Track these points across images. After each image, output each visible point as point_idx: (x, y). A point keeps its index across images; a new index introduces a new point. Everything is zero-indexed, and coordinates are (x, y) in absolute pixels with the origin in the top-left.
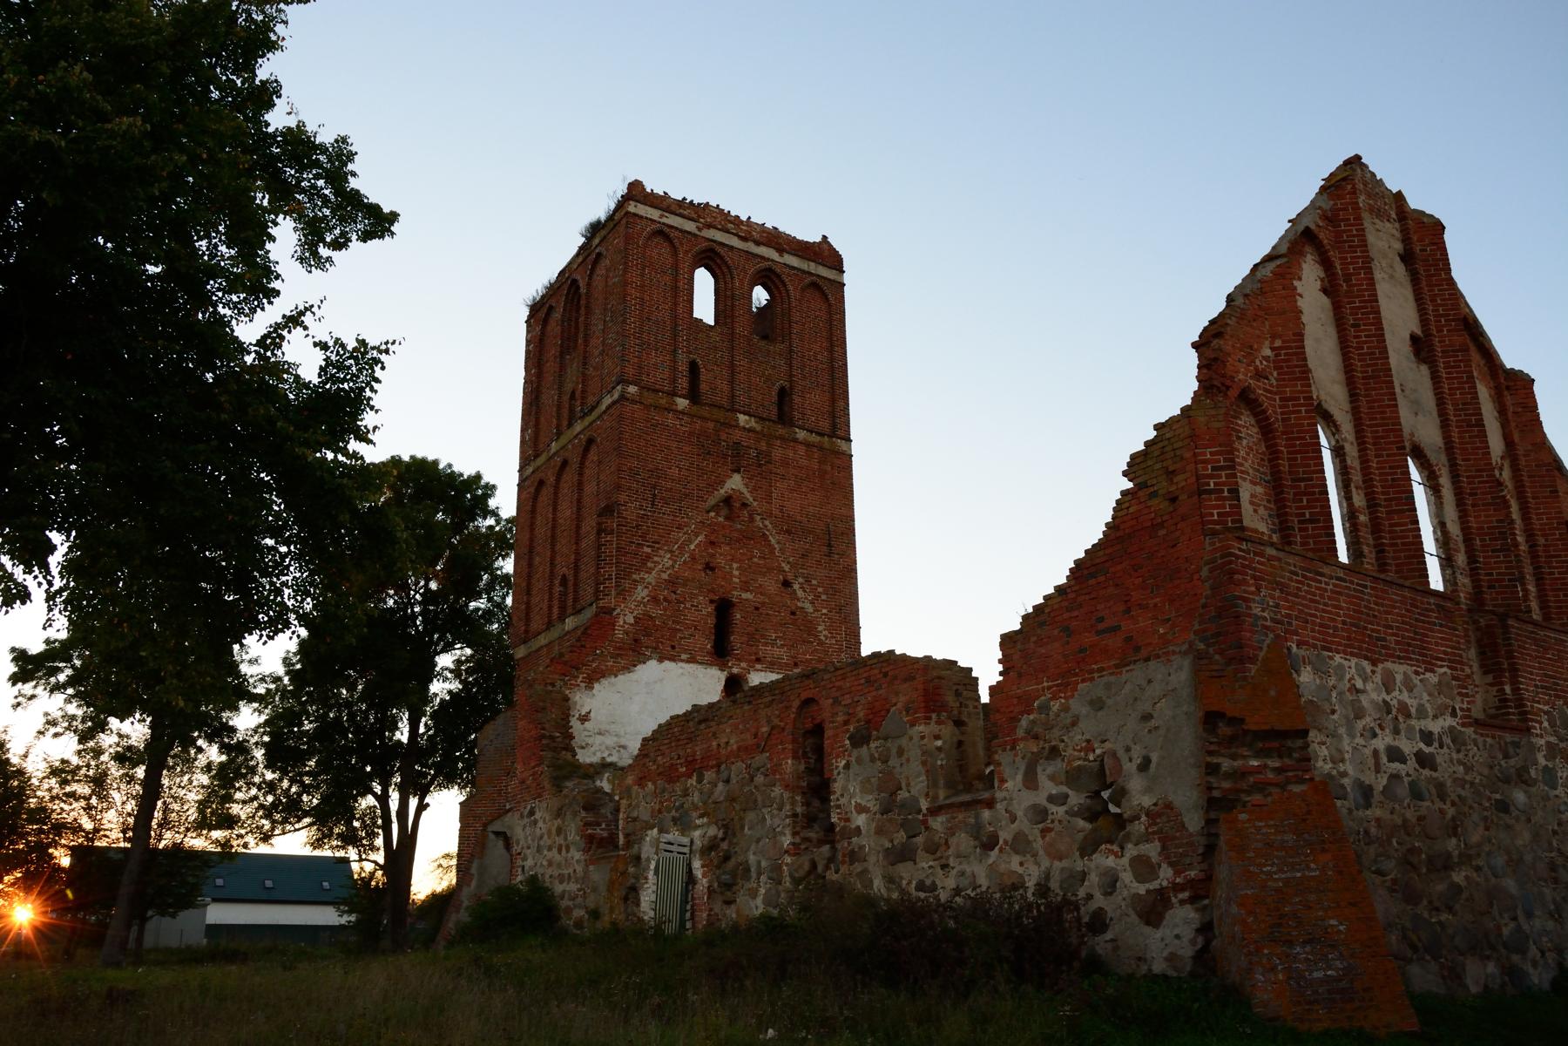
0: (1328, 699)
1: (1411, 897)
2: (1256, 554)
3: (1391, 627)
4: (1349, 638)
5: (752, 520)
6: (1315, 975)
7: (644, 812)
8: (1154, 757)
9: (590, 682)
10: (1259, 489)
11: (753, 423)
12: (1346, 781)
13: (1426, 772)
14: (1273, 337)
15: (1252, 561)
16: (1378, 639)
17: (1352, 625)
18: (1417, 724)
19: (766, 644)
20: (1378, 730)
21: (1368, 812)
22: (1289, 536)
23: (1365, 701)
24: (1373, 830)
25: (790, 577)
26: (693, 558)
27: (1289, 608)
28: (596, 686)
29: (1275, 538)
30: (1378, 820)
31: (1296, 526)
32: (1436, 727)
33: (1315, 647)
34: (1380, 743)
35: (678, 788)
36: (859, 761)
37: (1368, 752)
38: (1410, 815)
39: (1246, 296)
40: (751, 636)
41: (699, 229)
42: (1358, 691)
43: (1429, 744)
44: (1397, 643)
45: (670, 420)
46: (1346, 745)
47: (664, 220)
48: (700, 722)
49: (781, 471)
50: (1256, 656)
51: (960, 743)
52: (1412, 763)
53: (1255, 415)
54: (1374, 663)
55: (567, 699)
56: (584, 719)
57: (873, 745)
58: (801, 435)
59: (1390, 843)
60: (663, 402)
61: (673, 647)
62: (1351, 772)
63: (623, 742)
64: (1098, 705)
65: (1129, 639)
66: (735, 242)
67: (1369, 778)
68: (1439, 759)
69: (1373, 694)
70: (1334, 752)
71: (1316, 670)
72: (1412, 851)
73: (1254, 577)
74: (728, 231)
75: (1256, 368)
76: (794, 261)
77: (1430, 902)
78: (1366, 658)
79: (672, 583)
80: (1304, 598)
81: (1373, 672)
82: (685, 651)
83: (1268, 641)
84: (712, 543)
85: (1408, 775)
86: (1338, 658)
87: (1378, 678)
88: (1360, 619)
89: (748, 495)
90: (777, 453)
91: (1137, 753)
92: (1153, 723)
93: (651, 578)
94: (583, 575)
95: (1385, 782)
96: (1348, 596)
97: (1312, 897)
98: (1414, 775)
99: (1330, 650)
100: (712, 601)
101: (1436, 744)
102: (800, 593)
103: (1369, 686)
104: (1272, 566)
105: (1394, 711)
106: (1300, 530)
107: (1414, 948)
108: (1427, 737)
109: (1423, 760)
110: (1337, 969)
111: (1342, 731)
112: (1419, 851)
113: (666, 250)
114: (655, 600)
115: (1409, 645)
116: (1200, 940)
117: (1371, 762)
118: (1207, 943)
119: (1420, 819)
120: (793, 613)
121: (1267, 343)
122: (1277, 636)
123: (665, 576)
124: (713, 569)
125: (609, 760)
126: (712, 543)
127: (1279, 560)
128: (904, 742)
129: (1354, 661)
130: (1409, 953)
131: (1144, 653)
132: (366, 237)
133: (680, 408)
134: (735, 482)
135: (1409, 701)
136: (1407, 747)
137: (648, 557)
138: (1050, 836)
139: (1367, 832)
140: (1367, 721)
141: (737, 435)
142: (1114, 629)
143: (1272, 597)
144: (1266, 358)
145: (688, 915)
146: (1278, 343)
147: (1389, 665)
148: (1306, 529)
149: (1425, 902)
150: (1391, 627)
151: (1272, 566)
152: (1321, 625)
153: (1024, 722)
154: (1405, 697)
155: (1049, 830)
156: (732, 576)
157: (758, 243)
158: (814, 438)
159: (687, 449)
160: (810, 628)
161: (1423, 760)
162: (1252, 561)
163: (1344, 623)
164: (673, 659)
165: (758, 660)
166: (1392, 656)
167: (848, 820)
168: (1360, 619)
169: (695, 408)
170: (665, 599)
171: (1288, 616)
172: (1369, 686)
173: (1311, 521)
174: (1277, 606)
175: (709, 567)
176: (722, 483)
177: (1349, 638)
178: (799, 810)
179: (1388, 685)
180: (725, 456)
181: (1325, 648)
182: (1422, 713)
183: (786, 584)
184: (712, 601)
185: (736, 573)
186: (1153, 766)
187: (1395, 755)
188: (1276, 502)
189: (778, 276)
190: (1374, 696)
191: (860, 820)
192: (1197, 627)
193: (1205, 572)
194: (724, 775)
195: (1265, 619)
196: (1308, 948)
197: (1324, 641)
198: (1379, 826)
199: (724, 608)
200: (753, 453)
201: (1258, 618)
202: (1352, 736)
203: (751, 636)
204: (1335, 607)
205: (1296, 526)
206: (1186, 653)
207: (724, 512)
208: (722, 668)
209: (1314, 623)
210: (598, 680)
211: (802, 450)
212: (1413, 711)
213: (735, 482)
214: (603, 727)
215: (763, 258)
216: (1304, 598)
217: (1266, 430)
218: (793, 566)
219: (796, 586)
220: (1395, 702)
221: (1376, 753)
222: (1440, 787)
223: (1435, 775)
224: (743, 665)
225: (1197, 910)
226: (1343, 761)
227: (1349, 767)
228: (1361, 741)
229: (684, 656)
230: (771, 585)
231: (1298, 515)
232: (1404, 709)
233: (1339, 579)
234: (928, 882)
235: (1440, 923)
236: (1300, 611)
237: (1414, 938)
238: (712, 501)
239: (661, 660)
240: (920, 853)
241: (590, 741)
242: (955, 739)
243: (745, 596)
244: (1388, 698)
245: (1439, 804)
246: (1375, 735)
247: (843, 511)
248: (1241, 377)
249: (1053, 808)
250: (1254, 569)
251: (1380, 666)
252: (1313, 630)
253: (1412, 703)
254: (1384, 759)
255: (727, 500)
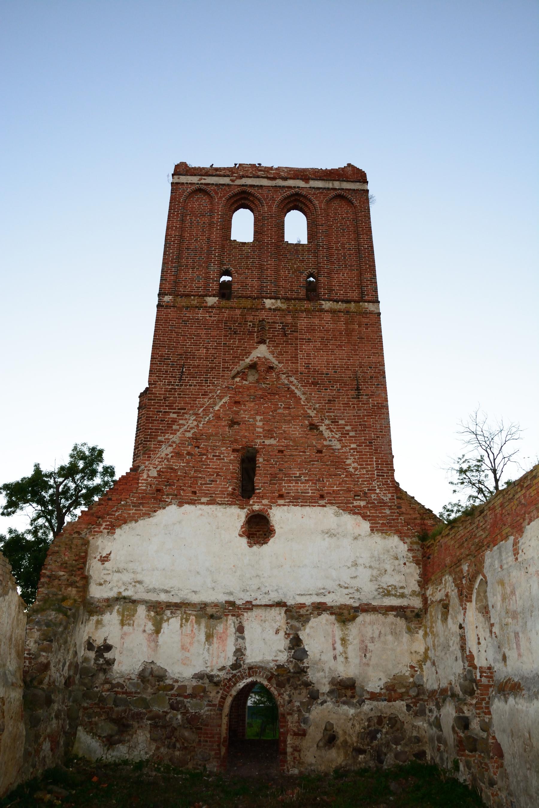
5: (278, 378)
9: (112, 528)
11: (279, 304)
25: (316, 421)
26: (218, 417)
28: (118, 531)
40: (274, 476)
41: (233, 181)
45: (201, 314)
47: (203, 181)
49: (308, 336)
55: (86, 543)
56: (104, 559)
58: (327, 305)
60: (195, 303)
63: (139, 577)
66: (265, 182)
74: (258, 177)
76: (319, 184)
82: (206, 495)
84: (237, 403)
89: (273, 360)
90: (303, 322)
93: (176, 438)
100: (234, 450)
102: (327, 434)
113: (205, 200)
114: (178, 455)
120: (320, 451)
123: (189, 435)
125: (125, 594)
126: (237, 403)
133: (209, 304)
134: (262, 351)
137: (174, 421)
141: (263, 315)
156: (254, 426)
157: (285, 179)
158: (341, 306)
159: (214, 333)
160: (338, 463)
164: (192, 502)
165: (281, 496)
169: (224, 303)
170: (189, 454)
180: (251, 333)
183: (313, 427)
185: (260, 424)
189: (305, 197)
200: (278, 326)
203: (274, 476)
210: (119, 526)
211: (328, 317)
213: (262, 351)
214: (121, 566)
215: (289, 187)
218: (320, 411)
219: (323, 428)
224: (265, 502)
229: (204, 500)
230: (296, 431)
238: (238, 368)
239: (180, 504)
241: (108, 578)
243: (267, 442)
247: (373, 359)
255: (253, 366)
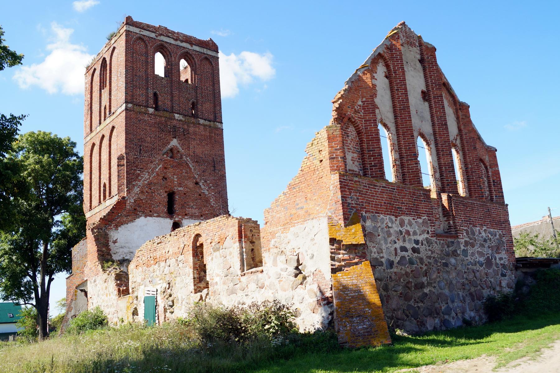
0: (377, 231)
1: (407, 298)
2: (350, 180)
3: (404, 203)
4: (386, 209)
5: (181, 158)
6: (360, 327)
7: (139, 280)
8: (315, 254)
9: (117, 227)
10: (355, 155)
11: (181, 117)
12: (383, 260)
13: (416, 254)
14: (363, 98)
15: (348, 183)
16: (398, 208)
17: (388, 203)
18: (413, 238)
19: (189, 208)
20: (397, 241)
21: (392, 270)
22: (366, 172)
23: (392, 231)
24: (393, 277)
25: (198, 180)
26: (158, 174)
27: (363, 199)
28: (119, 228)
29: (361, 173)
30: (395, 273)
31: (369, 168)
32: (420, 238)
33: (372, 212)
34: (398, 246)
35: (151, 269)
36: (216, 257)
37: (393, 249)
38: (408, 270)
39: (352, 82)
40: (183, 205)
41: (157, 36)
42: (389, 227)
43: (417, 244)
44: (406, 209)
45: (146, 118)
46: (384, 247)
47: (141, 33)
48: (158, 244)
49: (193, 137)
50: (348, 217)
51: (252, 250)
52: (410, 252)
53: (355, 127)
54: (396, 217)
55: (107, 235)
56: (115, 242)
57: (221, 251)
58: (202, 121)
59: (400, 280)
60: (143, 110)
61: (151, 211)
62: (385, 256)
63: (131, 250)
64: (297, 235)
65: (307, 212)
66: (172, 41)
67: (392, 258)
68: (421, 250)
69: (396, 228)
70: (379, 250)
71: (372, 221)
72: (409, 282)
73: (349, 189)
74: (169, 37)
75: (355, 109)
76: (197, 48)
77: (415, 300)
78: (393, 215)
79: (150, 184)
80: (369, 195)
81: (396, 220)
82: (156, 213)
83: (353, 212)
84: (166, 168)
85: (408, 256)
86: (382, 216)
87: (398, 222)
88: (391, 201)
89: (180, 148)
90: (191, 129)
91: (310, 252)
92: (314, 242)
93: (140, 183)
94: (112, 183)
95: (399, 259)
96: (387, 193)
97: (361, 301)
98: (411, 256)
99: (379, 213)
100: (166, 192)
101: (420, 244)
102: (203, 187)
103: (394, 225)
104: (357, 185)
105: (404, 234)
106: (370, 169)
107: (407, 316)
108: (417, 242)
109: (414, 250)
110: (367, 325)
111: (382, 242)
112: (411, 282)
113: (142, 45)
114: (142, 192)
115: (411, 209)
116: (330, 317)
117: (394, 252)
118: (332, 318)
119: (412, 271)
120: (200, 195)
121: (360, 100)
122: (357, 210)
123: (146, 182)
124: (166, 179)
125: (126, 258)
126: (166, 168)
127: (359, 182)
128: (231, 249)
129: (388, 216)
130: (405, 318)
131: (312, 217)
132: (11, 65)
133: (150, 113)
134: (174, 142)
135: (410, 230)
136: (409, 246)
137: (139, 175)
138: (282, 283)
139: (390, 277)
140: (393, 238)
141: (175, 122)
142: (302, 208)
143: (356, 195)
144: (360, 106)
145: (157, 318)
146: (364, 99)
147: (402, 217)
148: (372, 169)
149: (413, 300)
150: (404, 203)
151: (357, 185)
152: (375, 204)
153: (273, 242)
154: (408, 228)
155: (281, 281)
156: (174, 181)
157: (182, 41)
158: (207, 123)
159: (153, 129)
160: (207, 201)
161: (414, 250)
162: (348, 183)
163: (385, 203)
164: (150, 216)
165: (186, 215)
166: (404, 214)
167: (213, 279)
168: (391, 201)
169: (156, 112)
170: (147, 192)
171: (362, 202)
172: (394, 225)
173: (374, 166)
174: (358, 199)
175: (165, 178)
176: (169, 143)
177: (386, 209)
178: (196, 276)
179: (402, 224)
180: (170, 132)
181: (376, 213)
182: (415, 233)
183: (197, 183)
184: (166, 192)
185: (176, 180)
186: (314, 257)
187: (404, 249)
188: (362, 159)
189: (191, 55)
190: (396, 229)
191: (217, 279)
192: (328, 207)
193: (331, 188)
194: (168, 264)
195: (353, 204)
196: (358, 318)
197: (377, 210)
198: (396, 275)
199: (171, 196)
200: (181, 130)
201: (349, 204)
202: (386, 243)
203: (183, 205)
204: (381, 197)
205: (369, 168)
206: (325, 217)
207: (170, 155)
208: (171, 218)
209: (372, 204)
210: (120, 226)
211: (202, 128)
212: (411, 233)
213: (174, 142)
214: (123, 245)
215: (184, 47)
216: (369, 195)
217: (359, 133)
218: (199, 175)
219: (201, 184)
220: (404, 230)
221: (396, 249)
222: (421, 259)
223: (419, 255)
224: (180, 217)
225: (329, 307)
226: (382, 252)
227: (385, 255)
228: (390, 245)
229: (155, 215)
230: (191, 184)
231: (369, 164)
232: (408, 233)
233: (383, 187)
234: (241, 302)
235: (418, 307)
236: (367, 200)
237: (408, 313)
238: (165, 150)
239: (146, 217)
240: (239, 291)
241: (118, 251)
242: (250, 248)
243: (179, 189)
244: (401, 229)
245: (420, 265)
246: (395, 243)
247: (220, 152)
248: (349, 113)
249: (282, 273)
250: (349, 186)
251: (399, 218)
252: (372, 207)
253: (411, 230)
254: (399, 251)
255: (171, 150)
